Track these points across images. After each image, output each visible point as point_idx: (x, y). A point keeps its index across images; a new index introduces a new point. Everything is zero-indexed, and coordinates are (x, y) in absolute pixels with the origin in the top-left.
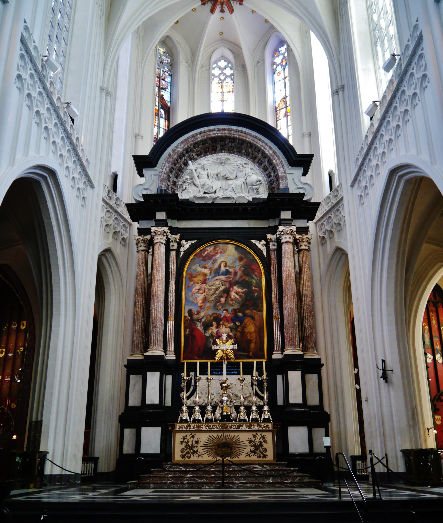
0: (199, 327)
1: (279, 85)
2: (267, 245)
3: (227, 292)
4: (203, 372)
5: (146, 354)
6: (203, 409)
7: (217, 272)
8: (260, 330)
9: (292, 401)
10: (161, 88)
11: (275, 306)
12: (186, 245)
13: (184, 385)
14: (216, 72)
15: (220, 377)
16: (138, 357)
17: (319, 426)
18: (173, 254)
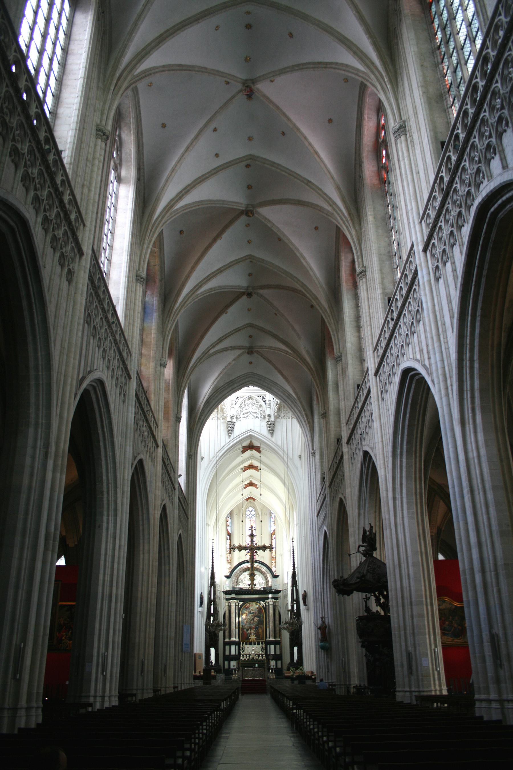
0: (245, 630)
1: (272, 524)
2: (265, 603)
3: (253, 619)
4: (246, 644)
5: (231, 640)
6: (246, 655)
7: (250, 613)
8: (263, 631)
9: (271, 653)
10: (227, 526)
11: (268, 624)
12: (241, 603)
13: (241, 648)
14: (248, 513)
15: (251, 646)
16: (227, 640)
17: (279, 660)
18: (237, 607)
